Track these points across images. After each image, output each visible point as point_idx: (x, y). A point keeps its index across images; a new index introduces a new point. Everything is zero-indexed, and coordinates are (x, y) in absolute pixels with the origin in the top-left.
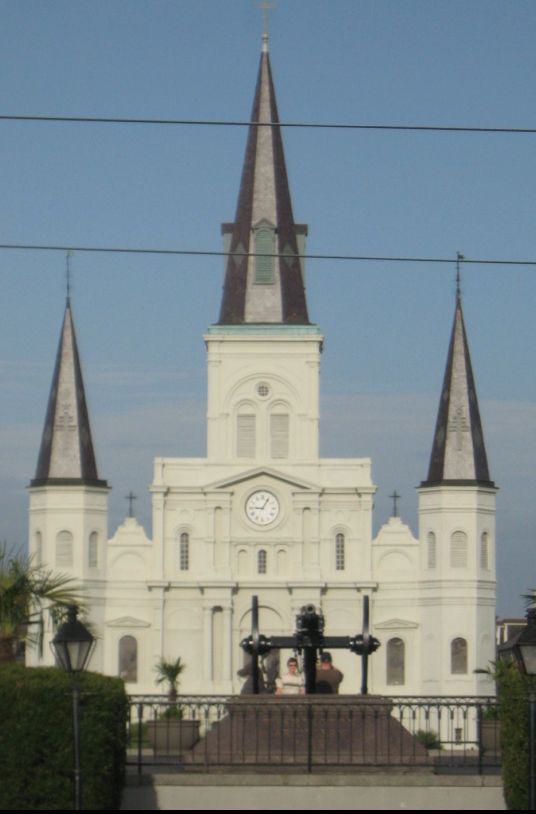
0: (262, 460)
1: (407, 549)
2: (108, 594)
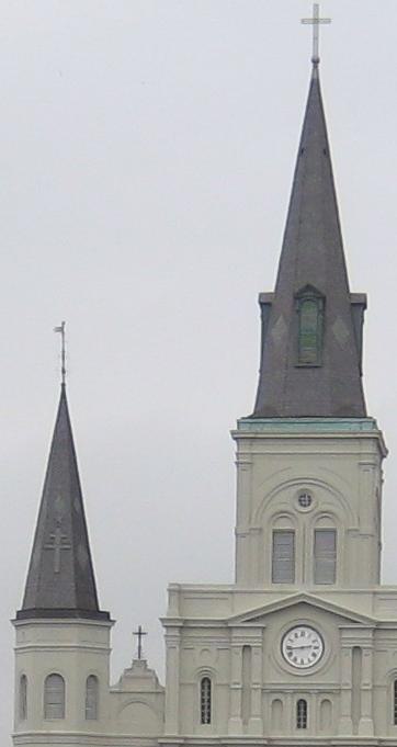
0: (299, 589)
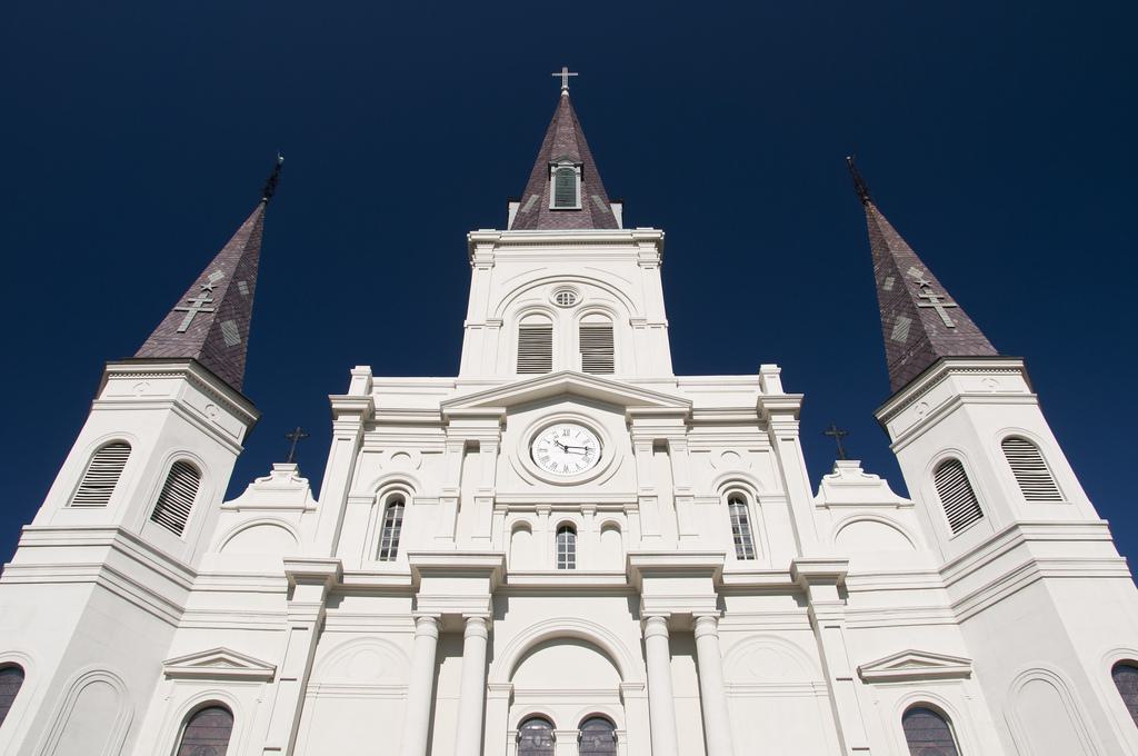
1: (890, 513)
2: (191, 602)
